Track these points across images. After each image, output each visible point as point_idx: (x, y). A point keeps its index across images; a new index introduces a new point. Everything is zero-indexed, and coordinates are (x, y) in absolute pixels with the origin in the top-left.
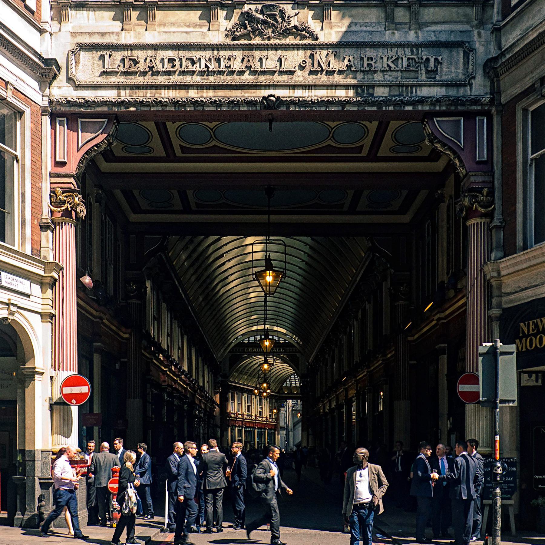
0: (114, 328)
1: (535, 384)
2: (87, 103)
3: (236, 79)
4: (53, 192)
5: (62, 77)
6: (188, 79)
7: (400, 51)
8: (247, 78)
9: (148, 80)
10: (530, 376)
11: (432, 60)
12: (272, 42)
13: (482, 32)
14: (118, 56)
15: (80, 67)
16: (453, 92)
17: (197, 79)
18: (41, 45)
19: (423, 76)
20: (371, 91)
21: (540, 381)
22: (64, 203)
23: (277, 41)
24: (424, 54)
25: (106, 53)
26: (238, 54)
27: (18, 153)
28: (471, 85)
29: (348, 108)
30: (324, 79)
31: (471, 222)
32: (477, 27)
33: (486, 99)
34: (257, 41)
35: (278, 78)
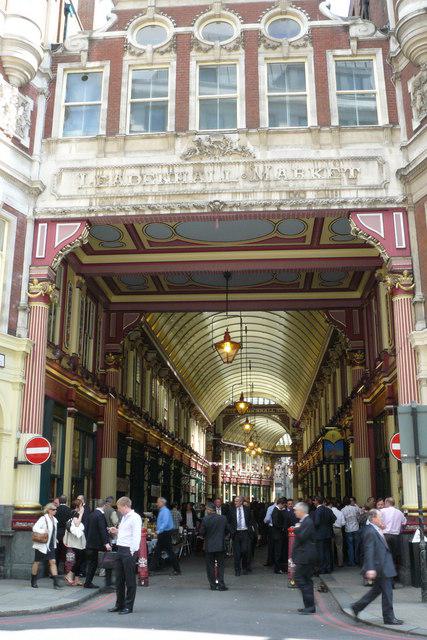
4: (31, 281)
5: (46, 194)
7: (324, 165)
8: (198, 187)
13: (393, 149)
14: (92, 176)
16: (373, 194)
17: (155, 189)
18: (30, 170)
19: (345, 183)
23: (222, 160)
24: (346, 166)
25: (82, 174)
31: (397, 299)
32: (388, 145)
33: (400, 199)
34: (205, 160)
35: (222, 186)
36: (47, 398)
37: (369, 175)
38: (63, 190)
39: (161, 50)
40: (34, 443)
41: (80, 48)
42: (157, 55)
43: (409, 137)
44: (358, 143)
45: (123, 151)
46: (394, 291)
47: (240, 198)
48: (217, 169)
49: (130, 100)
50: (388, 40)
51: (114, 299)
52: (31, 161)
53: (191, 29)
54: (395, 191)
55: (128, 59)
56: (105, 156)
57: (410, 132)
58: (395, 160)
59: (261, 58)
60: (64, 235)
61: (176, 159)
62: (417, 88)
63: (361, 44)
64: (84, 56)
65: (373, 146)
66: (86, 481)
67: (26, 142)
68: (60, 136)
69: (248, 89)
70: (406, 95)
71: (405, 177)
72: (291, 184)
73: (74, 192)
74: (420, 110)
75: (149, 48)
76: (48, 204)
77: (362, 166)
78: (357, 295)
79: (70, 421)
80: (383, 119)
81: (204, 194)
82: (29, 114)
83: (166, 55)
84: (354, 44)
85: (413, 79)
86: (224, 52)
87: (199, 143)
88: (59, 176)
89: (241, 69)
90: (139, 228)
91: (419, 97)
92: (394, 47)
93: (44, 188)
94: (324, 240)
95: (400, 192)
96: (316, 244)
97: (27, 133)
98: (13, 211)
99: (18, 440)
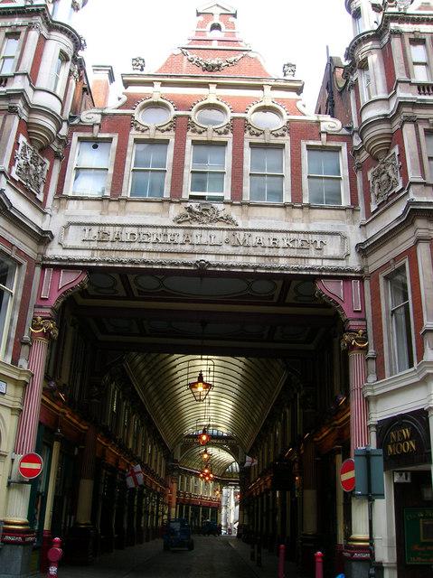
0: (75, 421)
1: (405, 481)
2: (69, 260)
3: (179, 248)
4: (35, 319)
5: (54, 244)
6: (143, 247)
8: (187, 248)
9: (115, 246)
10: (401, 475)
11: (319, 242)
12: (205, 226)
14: (95, 230)
15: (69, 236)
16: (333, 264)
17: (150, 247)
20: (275, 260)
21: (409, 479)
22: (42, 326)
23: (209, 226)
24: (315, 238)
25: (87, 228)
26: (181, 232)
27: (13, 292)
28: (347, 260)
29: (258, 271)
30: (241, 250)
33: (359, 269)
34: (195, 224)
35: (209, 249)
36: (40, 423)
37: (333, 248)
38: (69, 243)
39: (162, 128)
40: (27, 459)
41: (93, 120)
42: (159, 133)
43: (367, 218)
44: (323, 221)
45: (123, 211)
46: (351, 347)
47: (223, 260)
48: (204, 232)
49: (132, 168)
50: (351, 136)
51: (101, 337)
52: (45, 213)
53: (188, 113)
54: (354, 262)
55: (134, 134)
56: (108, 214)
57: (368, 213)
58: (356, 236)
59: (246, 144)
60: (66, 280)
61: (169, 222)
62: (376, 177)
63: (330, 136)
64: (96, 128)
65: (337, 223)
66: (65, 500)
67: (40, 197)
68: (70, 194)
69: (234, 166)
70: (366, 182)
71: (364, 250)
72: (267, 252)
73: (79, 244)
74: (377, 196)
75: (152, 127)
76: (54, 251)
77: (327, 239)
78: (312, 347)
79: (56, 445)
80: (345, 202)
81: (192, 253)
82: (45, 173)
83: (166, 133)
84: (324, 136)
85: (372, 170)
86: (215, 134)
87: (190, 210)
88: (66, 228)
89: (230, 147)
90: (131, 278)
91: (376, 185)
92: (357, 142)
93: (52, 237)
94: (290, 298)
95: (357, 263)
96: (281, 302)
97: (42, 189)
98: (26, 256)
99: (13, 460)
